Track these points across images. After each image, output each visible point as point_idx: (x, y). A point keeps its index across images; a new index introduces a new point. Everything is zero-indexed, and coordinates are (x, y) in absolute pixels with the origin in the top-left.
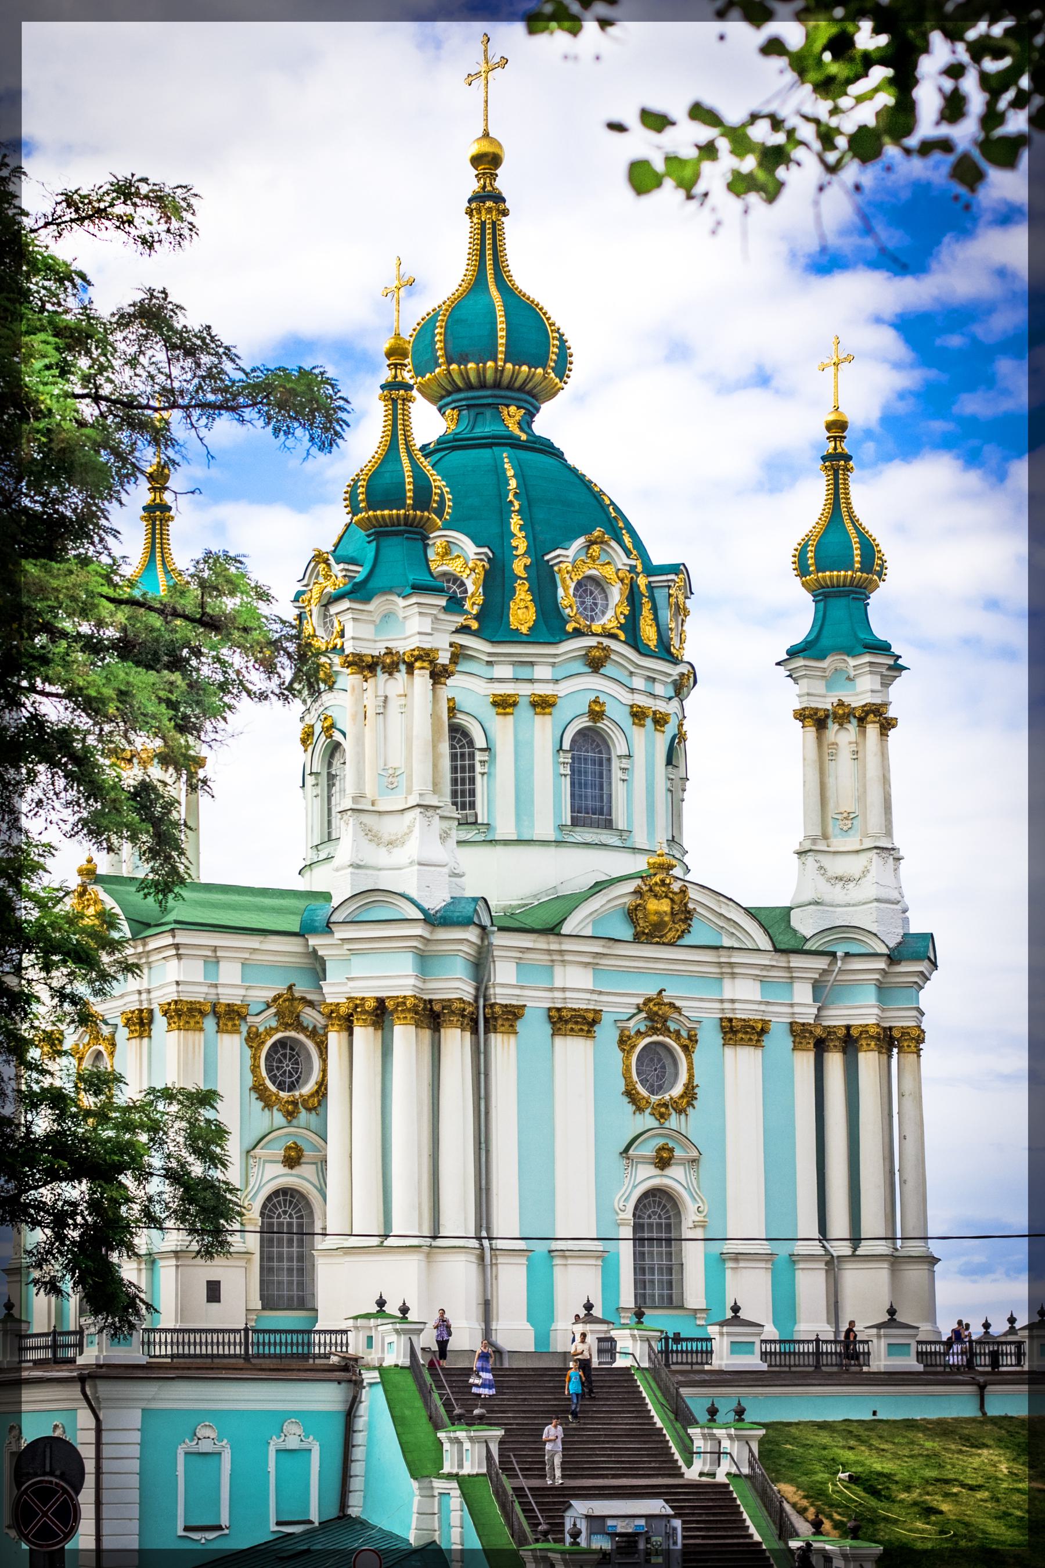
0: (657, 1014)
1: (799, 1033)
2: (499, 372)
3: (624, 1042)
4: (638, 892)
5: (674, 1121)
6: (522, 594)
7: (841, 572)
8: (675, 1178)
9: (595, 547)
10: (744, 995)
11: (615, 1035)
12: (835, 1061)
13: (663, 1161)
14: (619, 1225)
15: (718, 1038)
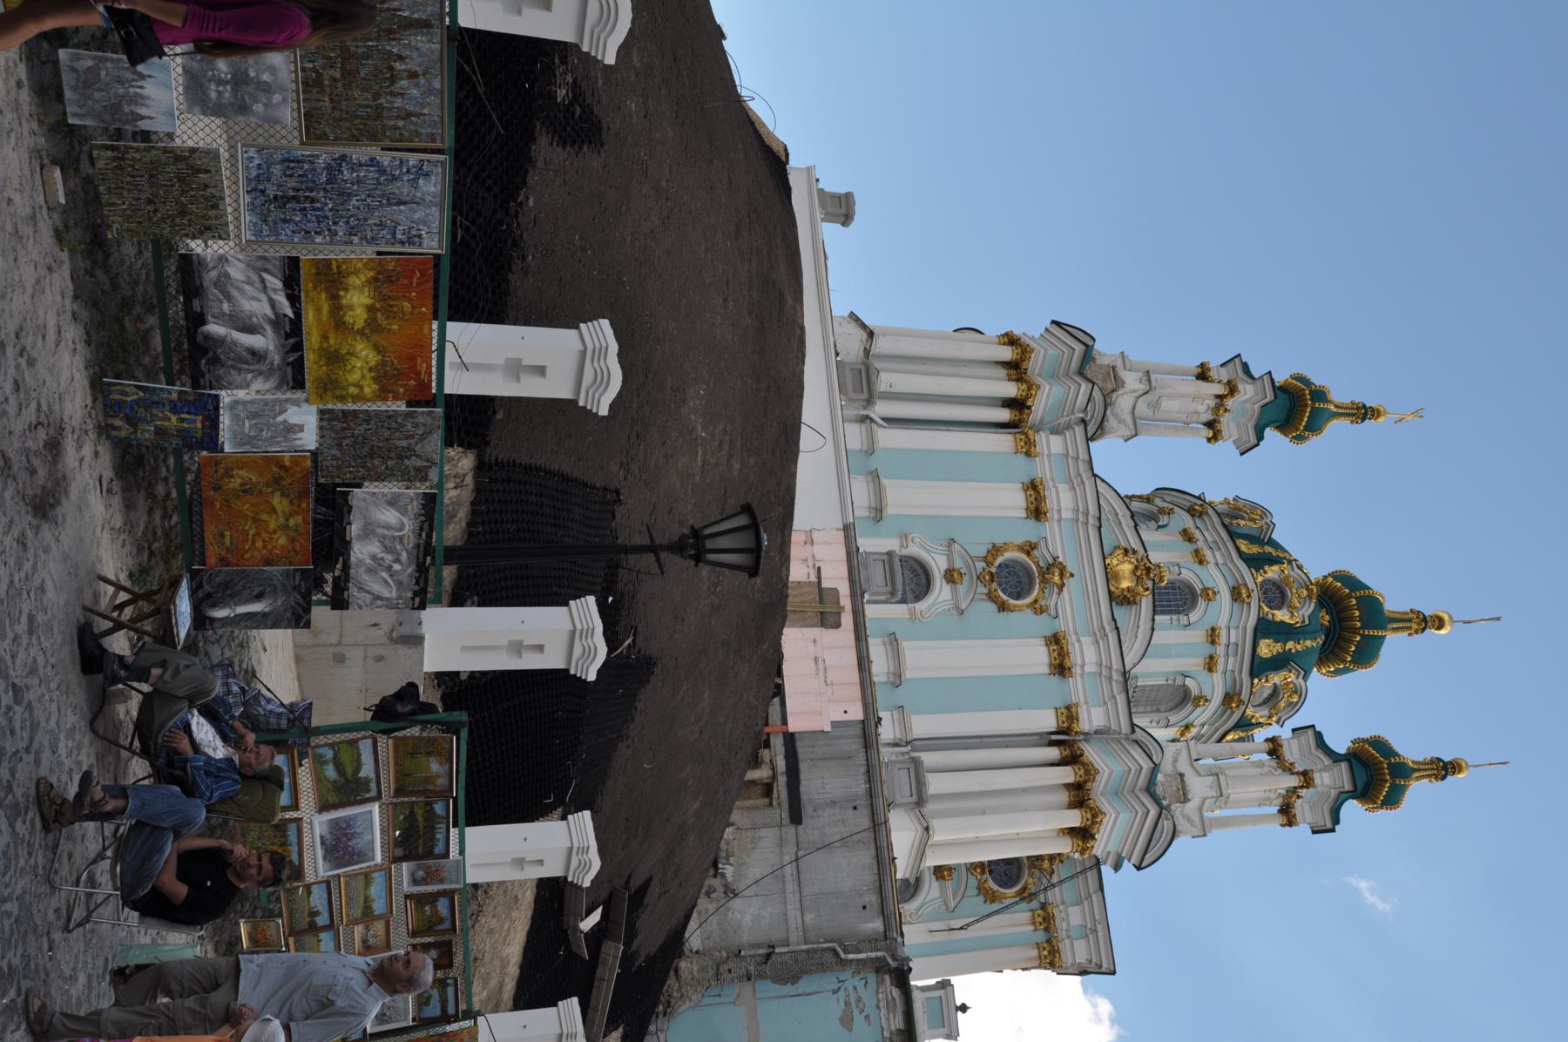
0: (1053, 572)
1: (1070, 713)
2: (1349, 597)
3: (1029, 548)
4: (1134, 552)
5: (982, 590)
6: (1255, 549)
7: (1375, 774)
8: (941, 592)
9: (1305, 593)
10: (1085, 654)
11: (1034, 540)
12: (1054, 753)
13: (951, 576)
14: (904, 537)
15: (1049, 633)
